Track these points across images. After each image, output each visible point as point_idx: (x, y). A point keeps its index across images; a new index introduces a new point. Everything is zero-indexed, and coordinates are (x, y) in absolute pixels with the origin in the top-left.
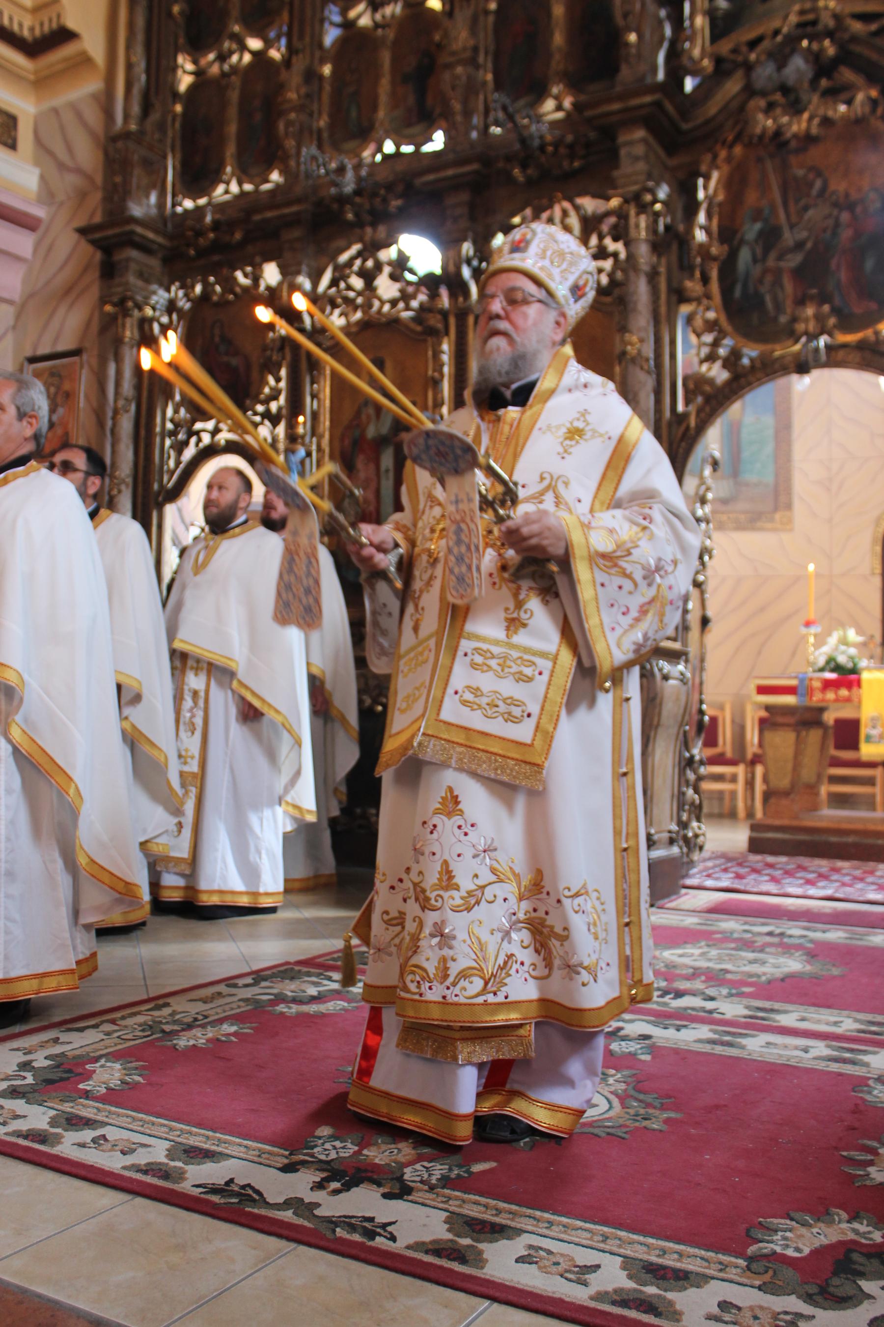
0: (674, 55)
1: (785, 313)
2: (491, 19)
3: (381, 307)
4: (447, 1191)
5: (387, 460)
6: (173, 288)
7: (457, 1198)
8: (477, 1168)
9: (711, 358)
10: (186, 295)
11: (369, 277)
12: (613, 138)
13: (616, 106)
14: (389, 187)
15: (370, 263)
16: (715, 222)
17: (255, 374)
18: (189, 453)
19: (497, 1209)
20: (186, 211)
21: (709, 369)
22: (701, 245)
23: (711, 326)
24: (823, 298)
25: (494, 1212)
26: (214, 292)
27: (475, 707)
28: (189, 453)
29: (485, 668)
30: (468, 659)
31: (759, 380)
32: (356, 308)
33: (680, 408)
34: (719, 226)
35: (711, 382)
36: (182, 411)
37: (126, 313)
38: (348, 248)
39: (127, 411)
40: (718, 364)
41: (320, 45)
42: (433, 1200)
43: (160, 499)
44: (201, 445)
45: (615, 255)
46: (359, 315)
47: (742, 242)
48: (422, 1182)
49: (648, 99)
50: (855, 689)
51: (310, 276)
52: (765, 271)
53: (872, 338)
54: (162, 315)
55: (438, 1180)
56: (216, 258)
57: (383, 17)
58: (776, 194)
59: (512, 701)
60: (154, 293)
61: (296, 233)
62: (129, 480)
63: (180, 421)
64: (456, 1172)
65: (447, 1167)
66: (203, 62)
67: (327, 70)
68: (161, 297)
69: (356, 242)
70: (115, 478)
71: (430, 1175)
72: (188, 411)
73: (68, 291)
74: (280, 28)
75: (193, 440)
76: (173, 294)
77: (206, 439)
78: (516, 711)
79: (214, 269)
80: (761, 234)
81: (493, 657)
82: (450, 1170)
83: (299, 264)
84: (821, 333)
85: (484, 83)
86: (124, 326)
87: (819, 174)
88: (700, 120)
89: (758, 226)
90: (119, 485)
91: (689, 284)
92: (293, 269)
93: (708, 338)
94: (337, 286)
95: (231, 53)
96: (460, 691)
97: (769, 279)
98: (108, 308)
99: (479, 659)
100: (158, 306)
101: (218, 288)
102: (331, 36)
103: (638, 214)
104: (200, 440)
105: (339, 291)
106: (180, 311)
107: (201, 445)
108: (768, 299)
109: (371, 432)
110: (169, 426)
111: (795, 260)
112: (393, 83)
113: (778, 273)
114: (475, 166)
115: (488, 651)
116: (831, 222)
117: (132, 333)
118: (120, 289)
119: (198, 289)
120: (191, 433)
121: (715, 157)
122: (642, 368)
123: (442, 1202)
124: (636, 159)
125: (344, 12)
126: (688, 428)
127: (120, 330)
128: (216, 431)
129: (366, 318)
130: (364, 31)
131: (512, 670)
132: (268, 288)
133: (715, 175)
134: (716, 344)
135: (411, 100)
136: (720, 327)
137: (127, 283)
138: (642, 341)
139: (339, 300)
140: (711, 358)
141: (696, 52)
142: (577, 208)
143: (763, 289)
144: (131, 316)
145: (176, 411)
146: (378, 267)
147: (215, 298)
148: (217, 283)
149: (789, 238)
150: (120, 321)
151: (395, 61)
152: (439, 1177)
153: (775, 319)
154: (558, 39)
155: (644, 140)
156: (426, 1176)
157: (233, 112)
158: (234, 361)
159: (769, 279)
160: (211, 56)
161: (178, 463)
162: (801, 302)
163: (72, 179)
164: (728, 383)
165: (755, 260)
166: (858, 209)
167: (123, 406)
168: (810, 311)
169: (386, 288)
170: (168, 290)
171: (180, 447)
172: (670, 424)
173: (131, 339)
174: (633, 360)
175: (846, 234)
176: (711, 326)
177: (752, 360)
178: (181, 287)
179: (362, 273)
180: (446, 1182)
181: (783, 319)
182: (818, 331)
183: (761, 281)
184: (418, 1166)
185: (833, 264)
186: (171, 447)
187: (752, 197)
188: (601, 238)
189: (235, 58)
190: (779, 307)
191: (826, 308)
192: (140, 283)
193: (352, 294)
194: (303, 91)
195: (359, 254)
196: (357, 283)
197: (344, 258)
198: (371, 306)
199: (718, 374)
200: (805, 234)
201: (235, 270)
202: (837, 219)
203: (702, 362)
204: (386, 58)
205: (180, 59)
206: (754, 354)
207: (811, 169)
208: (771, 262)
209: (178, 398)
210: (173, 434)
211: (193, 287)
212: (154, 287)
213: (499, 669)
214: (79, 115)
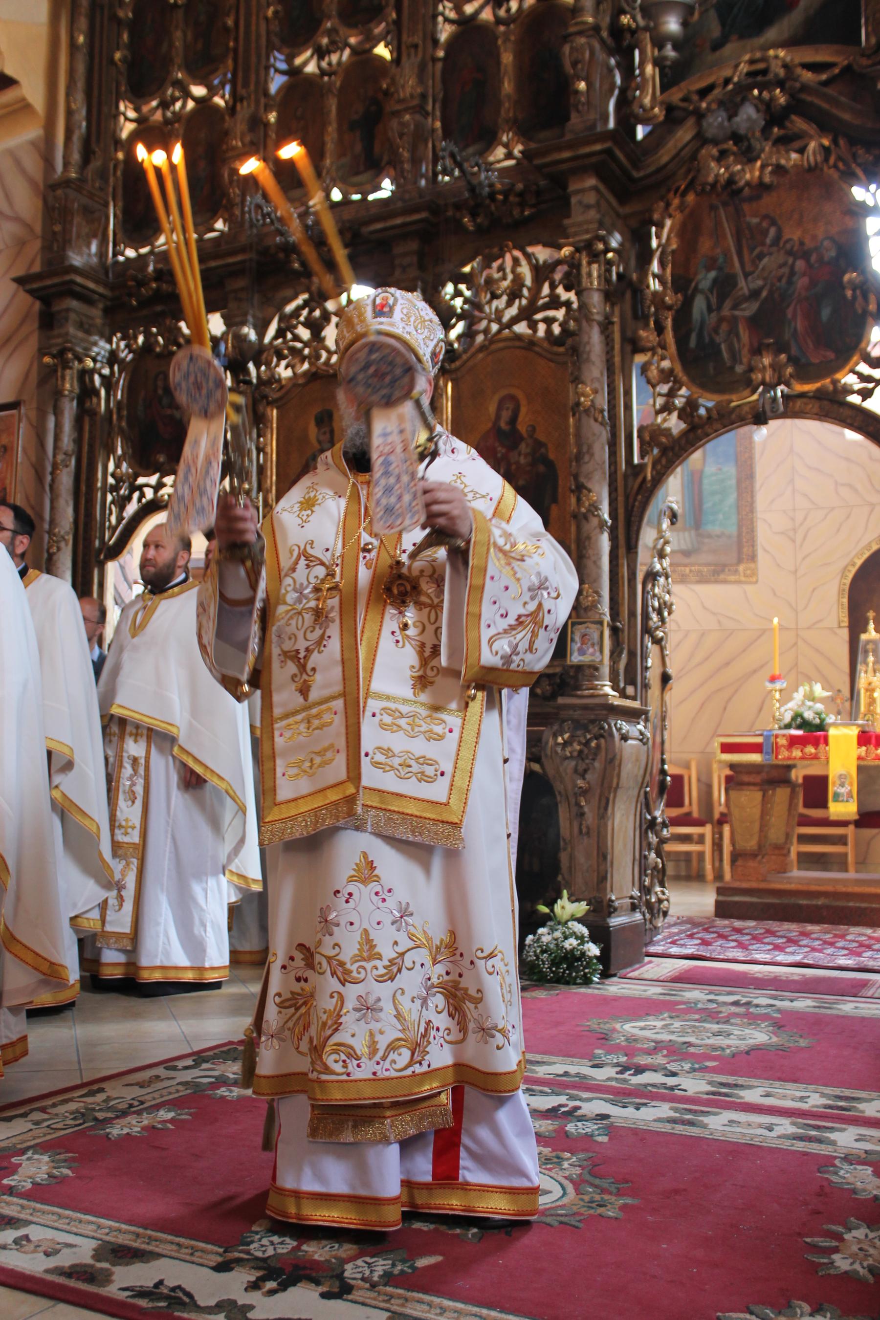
0: (624, 102)
1: (741, 363)
2: (439, 66)
3: (329, 359)
4: (389, 1289)
6: (115, 339)
7: (399, 1297)
8: (423, 1262)
9: (667, 408)
10: (127, 346)
11: (317, 328)
12: (565, 187)
13: (566, 155)
15: (317, 313)
16: (669, 271)
18: (132, 508)
19: (441, 1308)
20: (128, 259)
21: (665, 420)
22: (655, 293)
23: (666, 376)
24: (780, 348)
25: (438, 1311)
26: (157, 342)
27: (388, 768)
28: (132, 508)
29: (395, 728)
30: (377, 719)
31: (716, 431)
32: (303, 359)
33: (636, 461)
34: (672, 275)
35: (667, 432)
36: (124, 465)
37: (66, 365)
38: (295, 297)
39: (67, 466)
40: (675, 415)
41: (266, 93)
42: (375, 1299)
43: (102, 557)
44: (144, 500)
45: (568, 304)
46: (306, 366)
47: (696, 290)
48: (363, 1279)
49: (598, 147)
50: (822, 746)
51: (255, 327)
52: (721, 320)
53: (831, 388)
54: (102, 367)
55: (380, 1277)
56: (159, 308)
57: (330, 64)
58: (731, 242)
59: (424, 761)
60: (95, 344)
61: (241, 283)
62: (70, 538)
63: (122, 475)
64: (399, 1268)
65: (390, 1262)
66: (145, 109)
67: (272, 117)
68: (103, 348)
69: (303, 292)
70: (54, 535)
71: (372, 1272)
72: (130, 465)
74: (225, 75)
75: (136, 495)
76: (114, 346)
77: (149, 493)
78: (430, 771)
79: (156, 319)
80: (715, 281)
81: (402, 716)
82: (394, 1265)
83: (245, 314)
84: (779, 384)
85: (433, 130)
86: (63, 378)
87: (773, 223)
88: (652, 168)
89: (713, 274)
90: (58, 542)
91: (643, 333)
92: (238, 319)
93: (664, 388)
94: (284, 337)
95: (174, 100)
96: (371, 753)
97: (724, 327)
98: (47, 360)
99: (387, 719)
100: (99, 358)
101: (160, 339)
102: (276, 83)
103: (589, 264)
104: (142, 495)
105: (285, 342)
106: (122, 362)
107: (144, 500)
108: (723, 346)
110: (111, 480)
111: (750, 309)
112: (340, 130)
113: (733, 321)
114: (424, 215)
115: (397, 710)
116: (785, 270)
117: (72, 386)
118: (60, 340)
119: (141, 339)
120: (133, 488)
121: (668, 205)
122: (596, 420)
123: (384, 1301)
124: (588, 207)
125: (289, 60)
126: (644, 479)
127: (59, 382)
128: (160, 485)
129: (314, 370)
130: (310, 78)
131: (422, 729)
133: (668, 223)
134: (671, 394)
135: (358, 148)
136: (675, 377)
137: (67, 334)
138: (595, 392)
139: (286, 352)
140: (667, 408)
141: (647, 101)
142: (528, 256)
143: (718, 339)
144: (71, 368)
145: (118, 466)
146: (326, 317)
147: (158, 349)
148: (159, 334)
149: (743, 286)
150: (59, 374)
152: (381, 1273)
153: (732, 368)
154: (508, 87)
155: (595, 188)
156: (367, 1273)
159: (724, 327)
160: (154, 103)
161: (120, 519)
162: (757, 351)
164: (684, 434)
165: (710, 309)
166: (813, 258)
167: (63, 461)
168: (766, 361)
170: (110, 342)
171: (122, 503)
172: (625, 476)
173: (71, 391)
174: (587, 411)
175: (802, 282)
176: (666, 376)
177: (708, 410)
178: (123, 339)
179: (307, 324)
180: (388, 1278)
181: (739, 369)
182: (775, 381)
183: (716, 330)
184: (359, 1262)
185: (789, 313)
186: (112, 502)
187: (705, 245)
188: (553, 287)
189: (178, 105)
190: (735, 357)
191: (783, 357)
192: (80, 334)
193: (299, 345)
194: (248, 139)
195: (306, 304)
196: (304, 333)
197: (290, 308)
198: (319, 357)
199: (674, 424)
200: (760, 283)
201: (179, 320)
202: (792, 267)
203: (658, 413)
204: (332, 105)
205: (122, 107)
206: (710, 404)
207: (766, 217)
208: (726, 312)
209: (119, 452)
210: (115, 489)
211: (136, 338)
212: (96, 338)
213: (409, 728)
214: (18, 162)
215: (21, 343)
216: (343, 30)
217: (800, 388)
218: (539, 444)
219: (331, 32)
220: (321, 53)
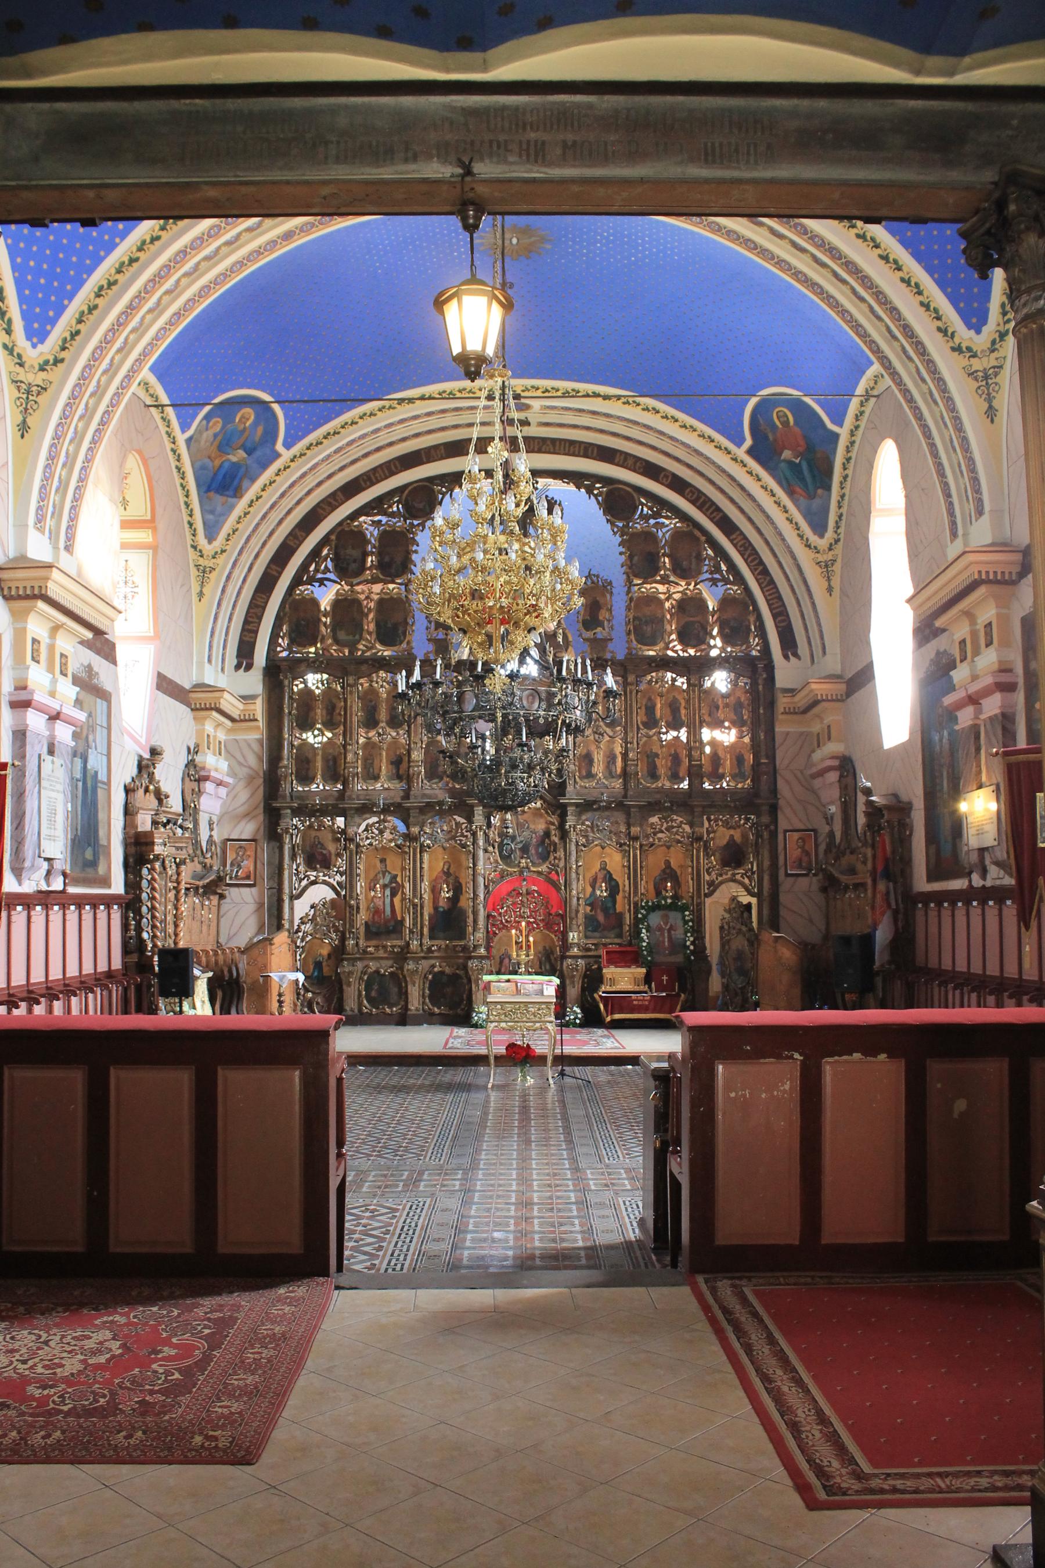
5: (388, 892)
14: (392, 804)
17: (333, 857)
18: (304, 883)
28: (304, 883)
73: (246, 815)
77: (313, 878)
102: (362, 740)
106: (299, 829)
109: (381, 882)
111: (520, 846)
125: (367, 733)
132: (339, 827)
145: (298, 866)
149: (518, 839)
151: (387, 754)
157: (319, 758)
158: (324, 852)
161: (299, 885)
162: (522, 858)
163: (245, 770)
168: (523, 861)
169: (387, 835)
171: (301, 880)
196: (377, 832)
204: (384, 753)
214: (249, 745)
215: (254, 817)
216: (388, 730)
217: (532, 869)
218: (457, 877)
219: (383, 728)
220: (379, 735)
